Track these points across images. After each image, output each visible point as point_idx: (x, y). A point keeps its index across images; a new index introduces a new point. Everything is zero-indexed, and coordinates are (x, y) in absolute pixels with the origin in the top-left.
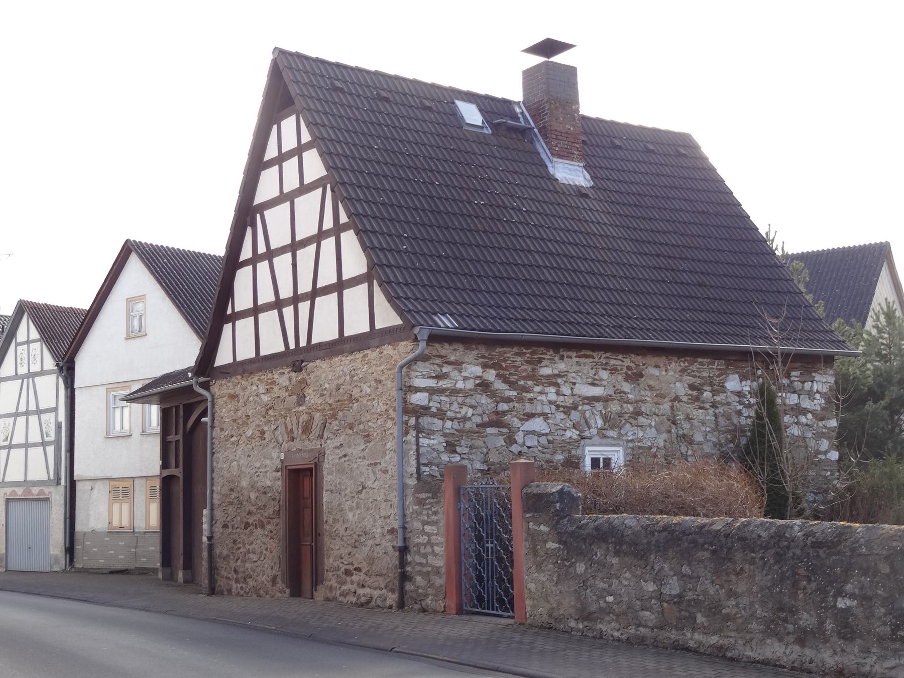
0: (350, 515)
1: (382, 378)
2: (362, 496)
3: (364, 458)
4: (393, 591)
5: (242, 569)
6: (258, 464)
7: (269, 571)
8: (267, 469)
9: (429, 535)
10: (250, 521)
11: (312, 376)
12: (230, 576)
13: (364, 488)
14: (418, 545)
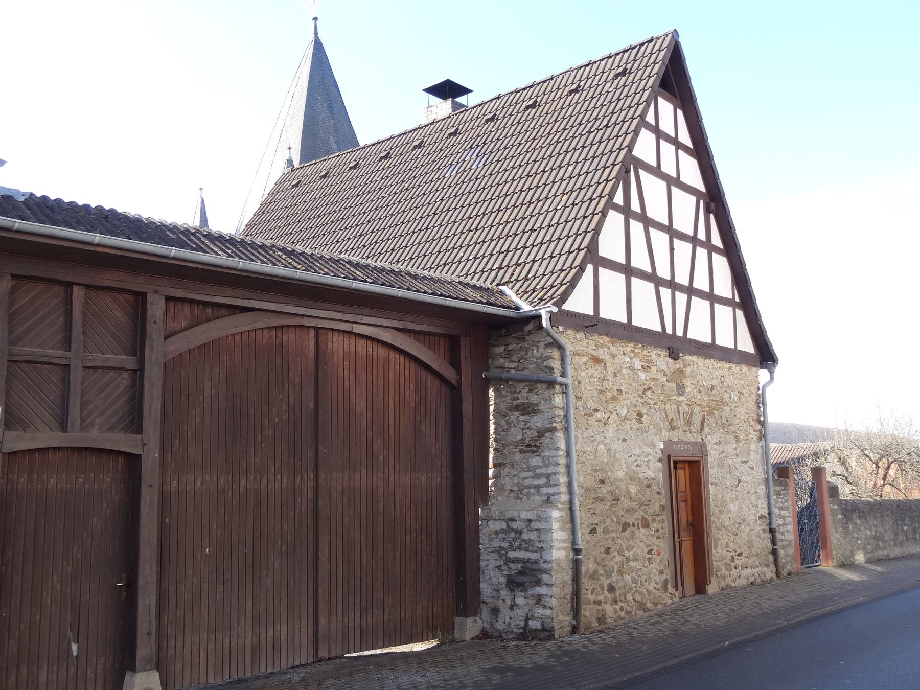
0: (732, 506)
1: (744, 391)
2: (739, 489)
3: (737, 455)
4: (767, 566)
5: (621, 584)
6: (637, 451)
7: (657, 578)
8: (650, 458)
9: (783, 517)
10: (631, 521)
11: (689, 369)
12: (601, 598)
13: (740, 481)
14: (779, 526)
